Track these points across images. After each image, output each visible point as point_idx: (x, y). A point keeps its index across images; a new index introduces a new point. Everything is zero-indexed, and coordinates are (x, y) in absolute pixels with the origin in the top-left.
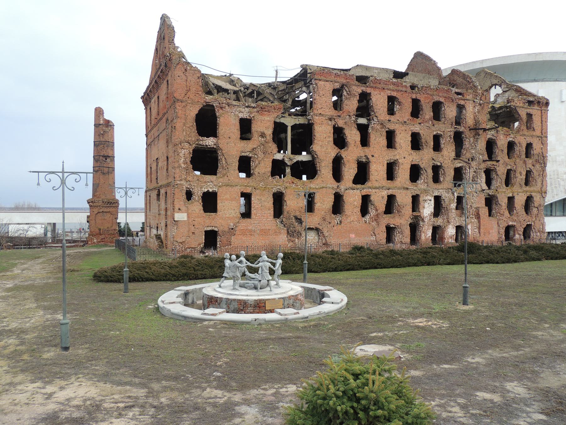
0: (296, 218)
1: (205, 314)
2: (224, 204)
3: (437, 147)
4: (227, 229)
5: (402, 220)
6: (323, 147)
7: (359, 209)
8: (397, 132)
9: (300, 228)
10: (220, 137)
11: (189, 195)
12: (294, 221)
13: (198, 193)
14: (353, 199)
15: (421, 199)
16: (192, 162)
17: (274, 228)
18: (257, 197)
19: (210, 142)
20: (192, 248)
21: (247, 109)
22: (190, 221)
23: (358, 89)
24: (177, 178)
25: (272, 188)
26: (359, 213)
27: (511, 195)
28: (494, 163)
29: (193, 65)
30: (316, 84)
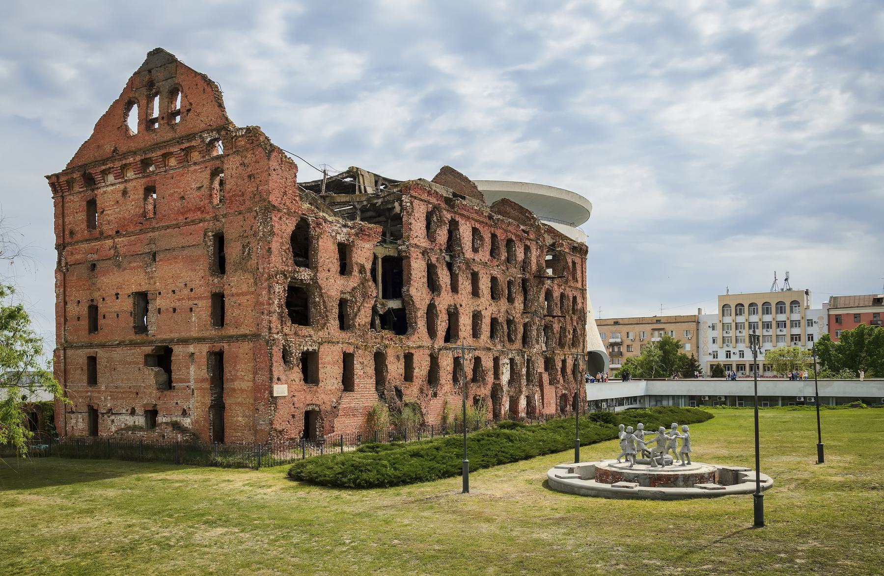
3: (511, 300)
4: (329, 408)
5: (485, 391)
6: (417, 290)
7: (450, 377)
8: (481, 276)
10: (320, 269)
11: (286, 355)
13: (296, 354)
14: (446, 363)
15: (501, 362)
16: (288, 304)
18: (360, 360)
19: (305, 274)
20: (292, 439)
21: (345, 230)
23: (448, 216)
24: (274, 331)
25: (373, 347)
27: (563, 358)
28: (551, 319)
29: (289, 156)
30: (411, 203)
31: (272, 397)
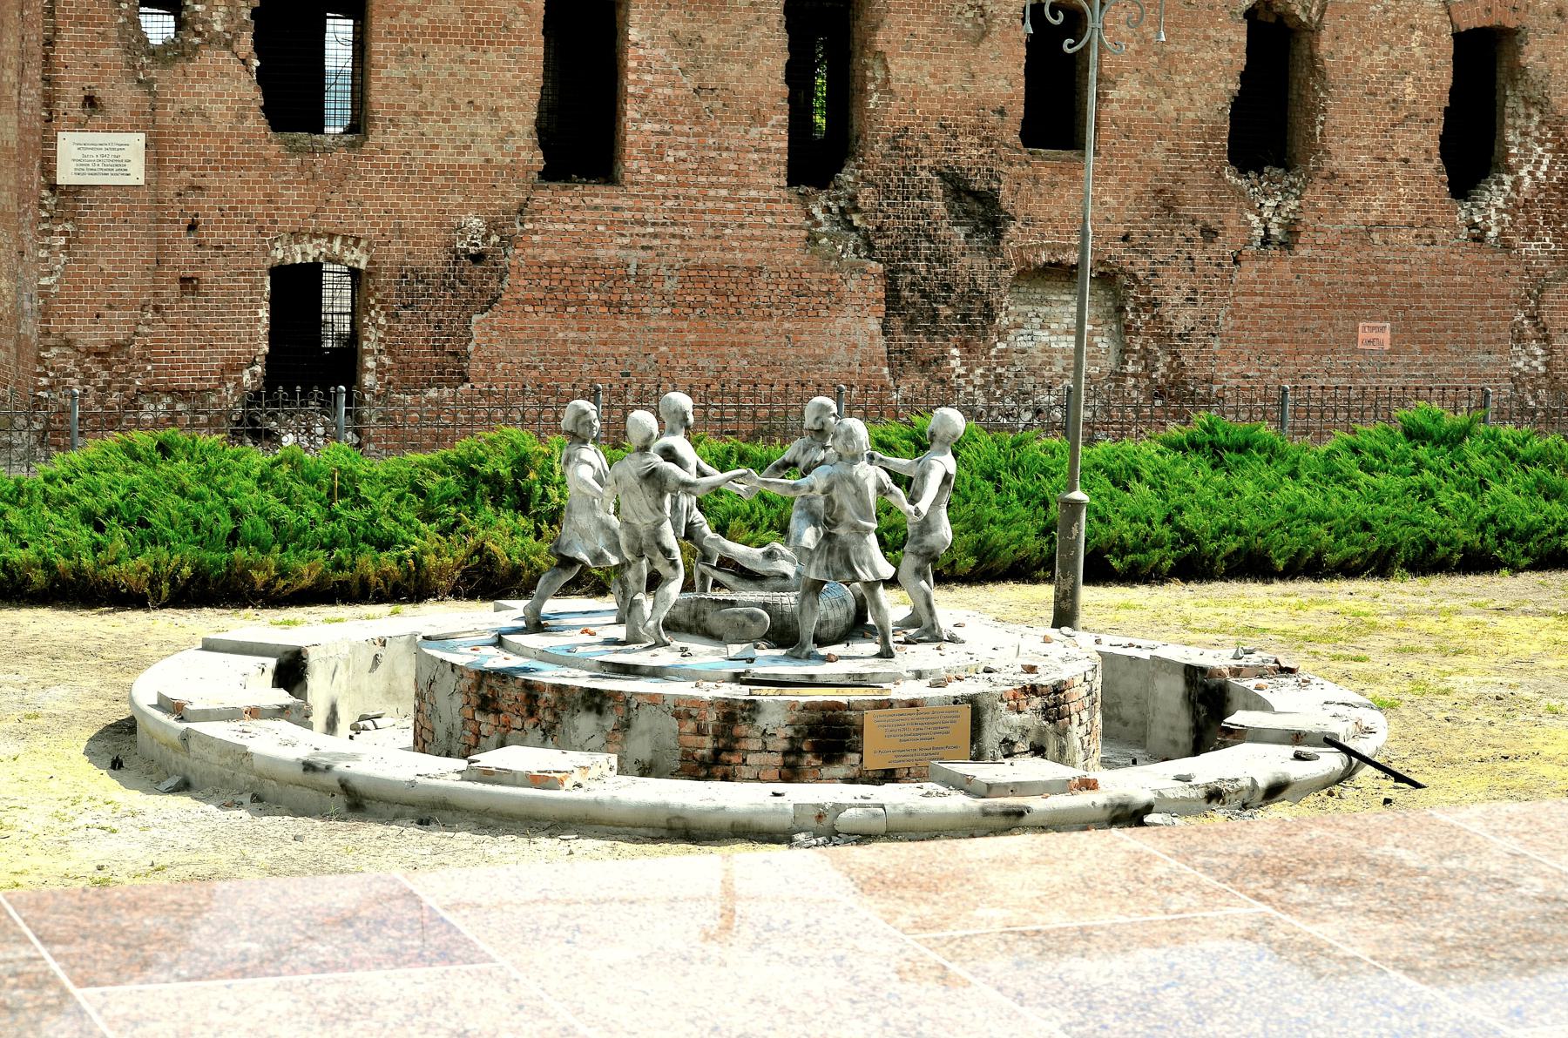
0: (957, 186)
1: (488, 776)
2: (418, 68)
4: (433, 260)
7: (1429, 137)
9: (981, 262)
12: (940, 207)
17: (793, 256)
20: (182, 394)
22: (169, 193)
26: (1432, 168)
31: (53, 187)
